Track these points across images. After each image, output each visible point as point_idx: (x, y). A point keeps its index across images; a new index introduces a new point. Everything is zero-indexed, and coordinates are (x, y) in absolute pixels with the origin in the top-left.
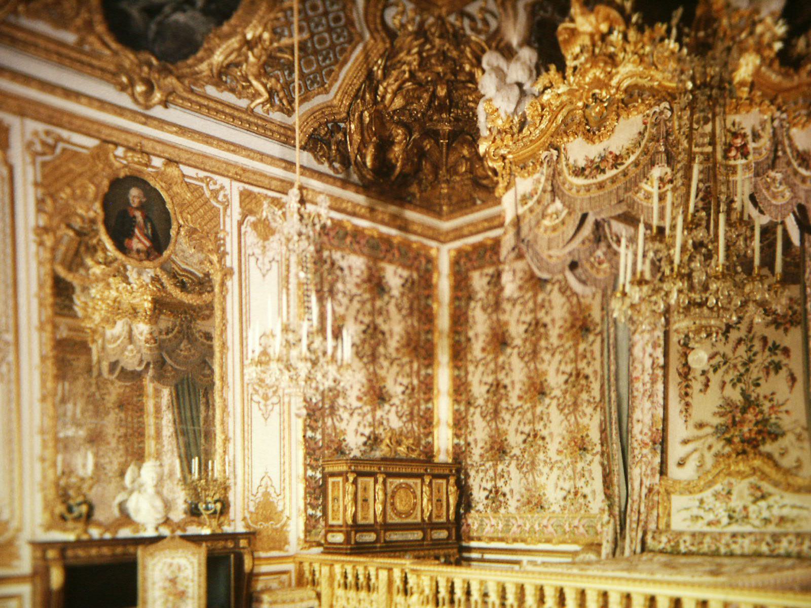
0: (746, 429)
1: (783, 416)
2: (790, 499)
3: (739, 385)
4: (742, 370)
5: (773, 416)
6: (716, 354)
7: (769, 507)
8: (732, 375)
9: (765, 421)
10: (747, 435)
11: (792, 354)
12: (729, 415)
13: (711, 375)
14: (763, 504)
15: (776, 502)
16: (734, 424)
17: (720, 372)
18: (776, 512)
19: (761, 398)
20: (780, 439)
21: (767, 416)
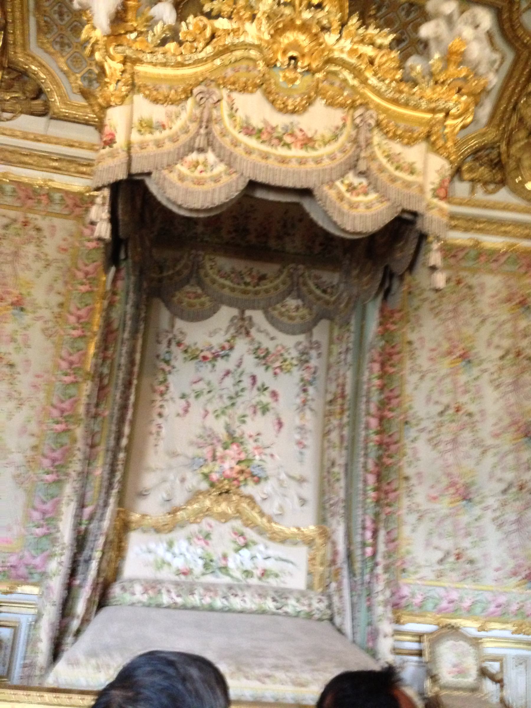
0: (227, 465)
1: (268, 459)
2: (276, 550)
3: (223, 419)
4: (228, 403)
5: (257, 457)
6: (200, 380)
7: (253, 558)
8: (217, 405)
9: (248, 461)
10: (228, 472)
11: (281, 399)
12: (209, 448)
13: (192, 400)
14: (245, 553)
15: (260, 552)
16: (214, 458)
17: (203, 399)
18: (262, 564)
19: (246, 436)
20: (263, 483)
21: (250, 456)
